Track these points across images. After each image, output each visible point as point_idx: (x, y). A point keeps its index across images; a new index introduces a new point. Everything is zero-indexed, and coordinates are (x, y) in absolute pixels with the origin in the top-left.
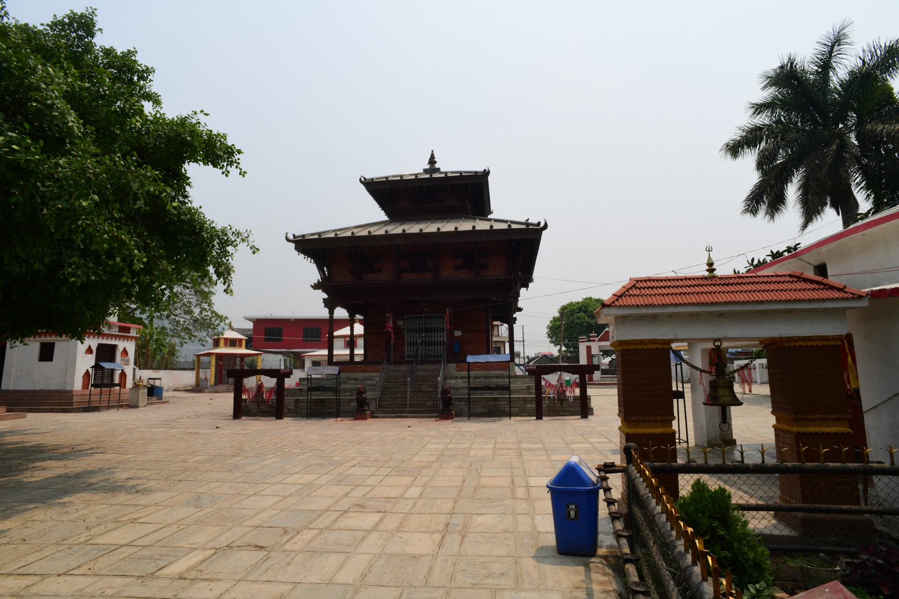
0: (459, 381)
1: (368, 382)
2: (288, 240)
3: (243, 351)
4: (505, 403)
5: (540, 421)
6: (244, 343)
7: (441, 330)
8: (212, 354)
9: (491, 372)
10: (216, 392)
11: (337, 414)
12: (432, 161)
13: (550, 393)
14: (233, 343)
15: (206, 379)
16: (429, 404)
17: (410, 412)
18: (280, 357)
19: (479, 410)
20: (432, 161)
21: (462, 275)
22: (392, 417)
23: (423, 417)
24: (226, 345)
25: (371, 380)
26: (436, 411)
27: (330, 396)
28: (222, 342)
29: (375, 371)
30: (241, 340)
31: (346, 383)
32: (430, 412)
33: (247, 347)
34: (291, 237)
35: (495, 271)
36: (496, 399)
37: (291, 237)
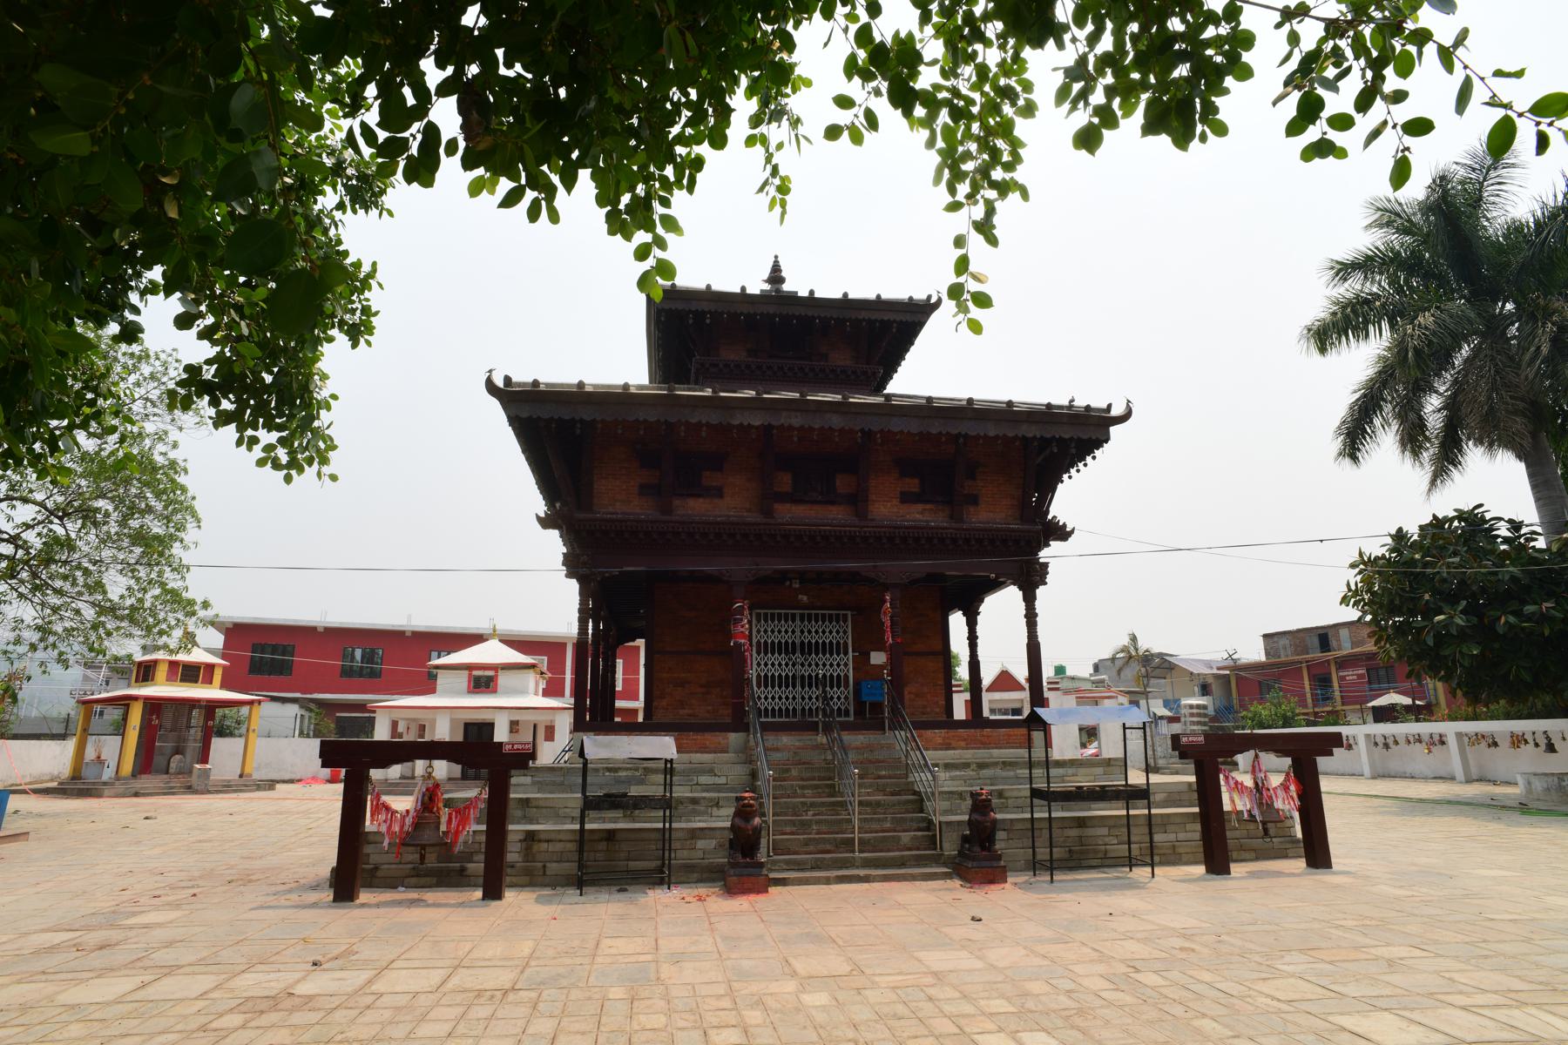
0: (943, 775)
1: (704, 779)
2: (491, 387)
3: (214, 692)
4: (1105, 831)
5: (1218, 882)
6: (218, 676)
7: (840, 649)
8: (135, 698)
9: (995, 752)
10: (136, 795)
11: (660, 877)
12: (776, 277)
13: (1232, 801)
14: (191, 673)
15: (99, 761)
16: (906, 837)
17: (867, 864)
18: (294, 709)
19: (1094, 862)
20: (776, 277)
21: (919, 515)
22: (828, 881)
23: (913, 878)
24: (171, 678)
25: (711, 772)
26: (937, 860)
27: (652, 822)
28: (161, 672)
29: (703, 749)
30: (210, 668)
31: (641, 782)
32: (920, 861)
33: (225, 685)
34: (500, 383)
35: (992, 513)
36: (1081, 823)
37: (500, 383)
